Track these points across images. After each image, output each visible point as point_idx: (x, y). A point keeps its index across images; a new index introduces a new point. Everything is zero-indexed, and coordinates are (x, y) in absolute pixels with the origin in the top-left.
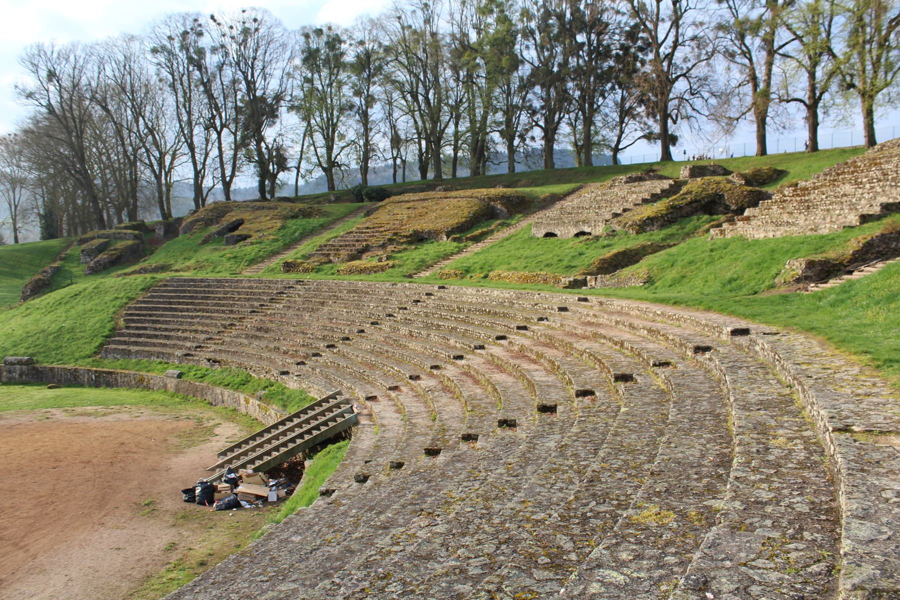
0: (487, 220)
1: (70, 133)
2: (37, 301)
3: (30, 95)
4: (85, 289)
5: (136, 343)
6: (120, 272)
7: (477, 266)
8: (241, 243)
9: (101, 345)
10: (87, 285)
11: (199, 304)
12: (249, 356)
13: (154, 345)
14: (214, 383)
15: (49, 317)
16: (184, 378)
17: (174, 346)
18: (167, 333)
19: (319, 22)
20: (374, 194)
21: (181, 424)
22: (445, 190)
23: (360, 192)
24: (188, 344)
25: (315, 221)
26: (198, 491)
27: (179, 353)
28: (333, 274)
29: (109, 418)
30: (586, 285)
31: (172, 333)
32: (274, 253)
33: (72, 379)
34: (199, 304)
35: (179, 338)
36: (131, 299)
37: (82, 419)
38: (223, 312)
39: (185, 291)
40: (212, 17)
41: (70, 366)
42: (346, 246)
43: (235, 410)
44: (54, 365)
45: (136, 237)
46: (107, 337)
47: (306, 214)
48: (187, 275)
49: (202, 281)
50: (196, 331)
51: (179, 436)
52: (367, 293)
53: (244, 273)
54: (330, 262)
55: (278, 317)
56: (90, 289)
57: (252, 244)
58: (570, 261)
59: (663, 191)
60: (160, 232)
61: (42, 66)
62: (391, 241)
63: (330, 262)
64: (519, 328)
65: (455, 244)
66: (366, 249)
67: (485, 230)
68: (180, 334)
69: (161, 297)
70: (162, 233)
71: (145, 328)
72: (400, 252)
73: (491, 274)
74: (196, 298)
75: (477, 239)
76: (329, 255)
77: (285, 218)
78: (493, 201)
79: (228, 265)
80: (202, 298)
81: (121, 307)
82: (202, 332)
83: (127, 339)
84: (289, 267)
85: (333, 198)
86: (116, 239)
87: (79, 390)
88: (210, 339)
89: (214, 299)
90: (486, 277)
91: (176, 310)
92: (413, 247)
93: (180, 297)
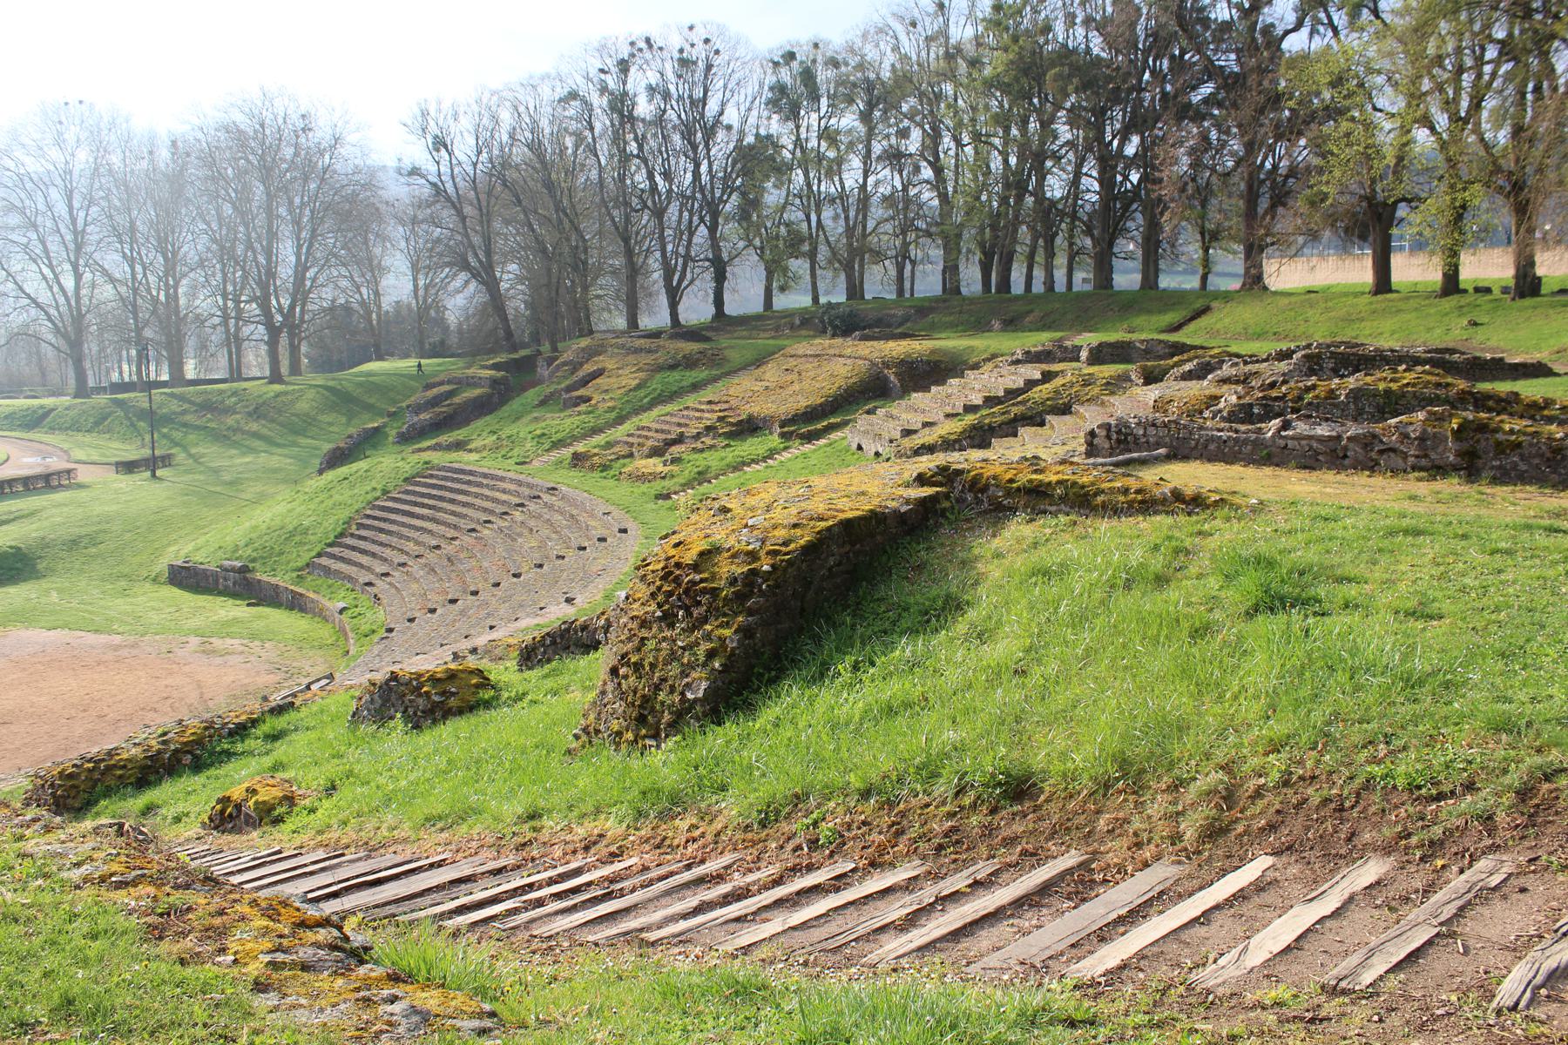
40: (648, 41)
42: (663, 431)
54: (631, 455)
57: (579, 413)
62: (708, 428)
72: (702, 451)
76: (632, 445)
77: (660, 368)
78: (888, 367)
84: (578, 459)
85: (797, 322)
86: (469, 385)
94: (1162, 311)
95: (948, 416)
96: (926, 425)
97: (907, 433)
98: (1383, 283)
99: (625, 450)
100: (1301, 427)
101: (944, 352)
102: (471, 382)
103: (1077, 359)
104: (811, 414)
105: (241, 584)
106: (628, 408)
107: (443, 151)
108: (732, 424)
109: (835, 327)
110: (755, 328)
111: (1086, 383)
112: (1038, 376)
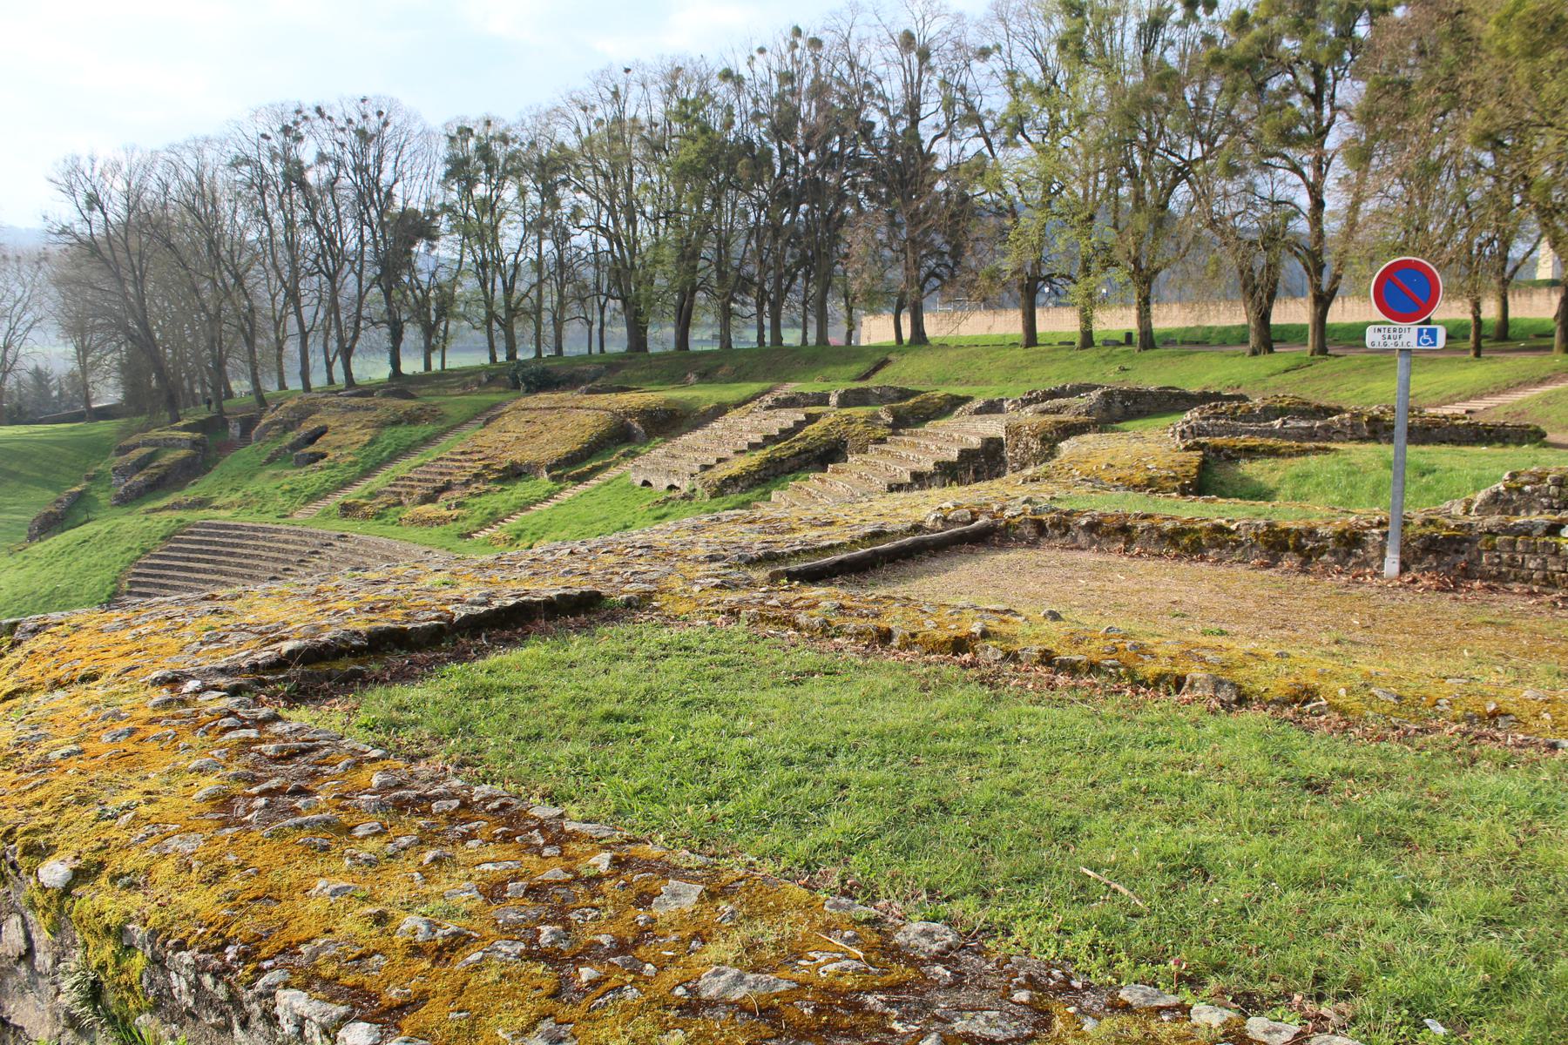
6: (149, 506)
7: (532, 529)
8: (310, 467)
10: (97, 528)
19: (473, 115)
20: (532, 379)
22: (590, 392)
25: (427, 429)
36: (145, 551)
40: (319, 110)
42: (426, 480)
47: (412, 419)
48: (223, 516)
49: (236, 528)
53: (298, 516)
54: (400, 503)
57: (322, 468)
59: (782, 431)
61: (79, 190)
62: (477, 476)
63: (400, 503)
70: (238, 433)
72: (479, 495)
77: (383, 425)
79: (281, 500)
81: (131, 562)
84: (347, 510)
85: (484, 379)
86: (167, 446)
89: (240, 555)
91: (191, 570)
92: (499, 487)
94: (851, 363)
95: (736, 452)
96: (719, 461)
97: (706, 468)
98: (1031, 338)
99: (394, 499)
100: (1292, 423)
101: (677, 402)
102: (171, 444)
103: (827, 404)
104: (572, 460)
106: (370, 462)
107: (98, 212)
108: (498, 471)
109: (528, 383)
110: (438, 386)
111: (850, 422)
112: (802, 417)
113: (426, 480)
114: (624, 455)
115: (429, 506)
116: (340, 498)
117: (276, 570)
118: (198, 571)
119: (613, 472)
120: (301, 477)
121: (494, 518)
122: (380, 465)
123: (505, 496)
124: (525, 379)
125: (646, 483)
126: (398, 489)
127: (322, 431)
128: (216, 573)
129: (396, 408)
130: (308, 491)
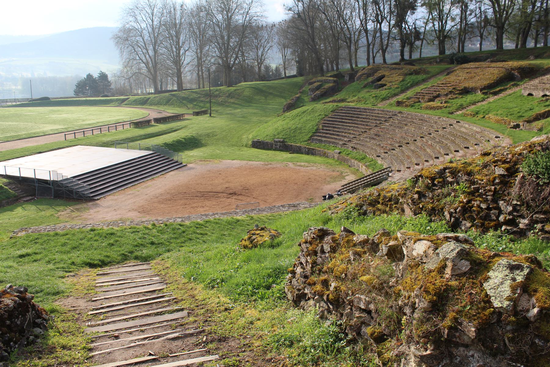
0: (508, 81)
1: (307, 26)
2: (288, 113)
3: (290, 9)
4: (308, 110)
5: (325, 137)
7: (483, 111)
8: (381, 89)
9: (311, 136)
10: (307, 108)
11: (354, 120)
12: (368, 147)
13: (332, 138)
14: (352, 158)
15: (292, 122)
16: (341, 154)
17: (340, 139)
18: (338, 133)
20: (459, 60)
21: (334, 173)
22: (492, 62)
23: (452, 57)
24: (346, 139)
26: (327, 197)
27: (341, 143)
28: (418, 109)
29: (308, 168)
30: (519, 128)
31: (340, 134)
32: (396, 95)
33: (298, 150)
34: (354, 120)
35: (342, 136)
36: (326, 116)
37: (298, 168)
38: (364, 125)
39: (349, 113)
41: (298, 145)
42: (429, 93)
43: (358, 170)
44: (292, 144)
45: (335, 82)
46: (314, 133)
47: (417, 73)
48: (352, 105)
49: (358, 108)
50: (350, 133)
51: (331, 178)
52: (427, 121)
53: (379, 106)
54: (419, 102)
55: (386, 129)
56: (310, 110)
57: (386, 89)
58: (523, 113)
60: (347, 78)
62: (451, 92)
63: (419, 102)
64: (465, 148)
65: (482, 96)
66: (435, 97)
67: (503, 88)
68: (343, 134)
69: (339, 115)
70: (348, 79)
71: (330, 130)
72: (453, 99)
73: (487, 116)
74: (354, 117)
75: (495, 94)
76: (419, 98)
77: (406, 75)
78: (514, 70)
79: (372, 100)
80: (356, 117)
81: (321, 119)
82: (352, 134)
83: (321, 134)
84: (399, 103)
85: (438, 60)
86: (326, 82)
87: (300, 155)
88: (355, 137)
89: (361, 118)
90: (484, 117)
91: (344, 122)
92: (461, 96)
93: (346, 116)
101: (534, 65)
102: (327, 82)
105: (283, 146)
110: (420, 63)
113: (429, 93)
114: (512, 85)
115: (432, 103)
116: (395, 99)
117: (376, 123)
118: (346, 123)
119: (509, 92)
120: (378, 92)
121: (461, 107)
122: (407, 89)
123: (464, 99)
124: (456, 60)
125: (530, 95)
126: (418, 96)
127: (383, 77)
128: (354, 123)
129: (410, 70)
130: (382, 97)
